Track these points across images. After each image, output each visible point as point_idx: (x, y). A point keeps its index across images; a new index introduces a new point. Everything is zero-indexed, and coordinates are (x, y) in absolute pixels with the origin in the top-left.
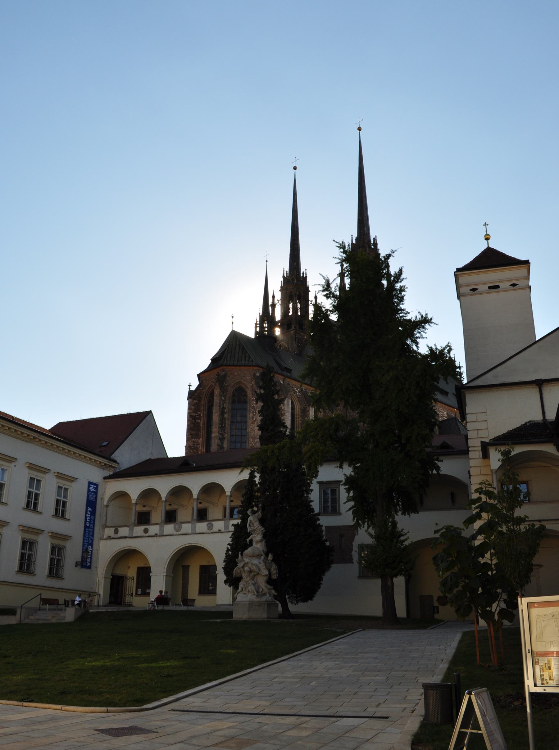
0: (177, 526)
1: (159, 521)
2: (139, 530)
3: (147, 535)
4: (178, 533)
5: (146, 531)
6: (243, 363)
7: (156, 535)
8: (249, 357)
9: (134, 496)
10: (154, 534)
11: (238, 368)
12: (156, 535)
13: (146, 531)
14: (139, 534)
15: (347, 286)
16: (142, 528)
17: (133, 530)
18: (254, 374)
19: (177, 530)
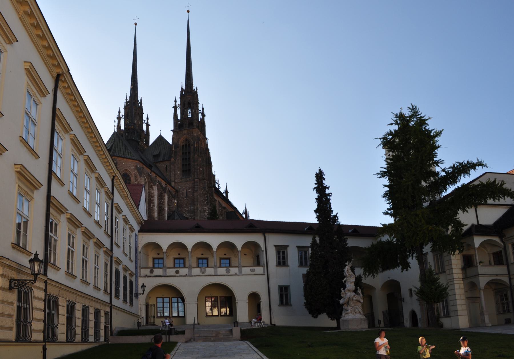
0: (203, 270)
1: (172, 266)
2: (172, 272)
3: (178, 275)
4: (203, 274)
5: (177, 272)
6: (128, 156)
7: (186, 276)
8: (131, 153)
9: (165, 247)
10: (234, 274)
11: (125, 159)
12: (186, 276)
13: (177, 272)
14: (172, 274)
15: (179, 118)
16: (175, 270)
17: (166, 271)
18: (136, 166)
19: (203, 273)
